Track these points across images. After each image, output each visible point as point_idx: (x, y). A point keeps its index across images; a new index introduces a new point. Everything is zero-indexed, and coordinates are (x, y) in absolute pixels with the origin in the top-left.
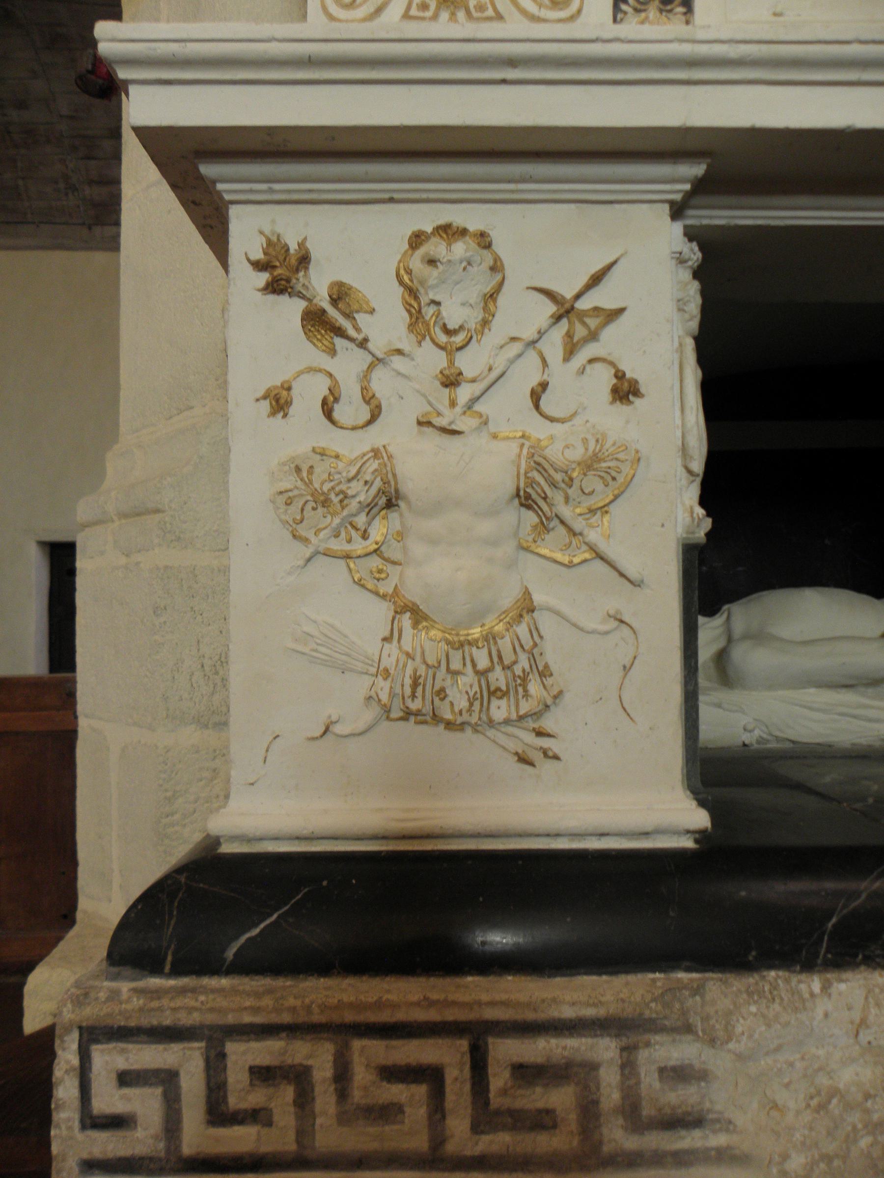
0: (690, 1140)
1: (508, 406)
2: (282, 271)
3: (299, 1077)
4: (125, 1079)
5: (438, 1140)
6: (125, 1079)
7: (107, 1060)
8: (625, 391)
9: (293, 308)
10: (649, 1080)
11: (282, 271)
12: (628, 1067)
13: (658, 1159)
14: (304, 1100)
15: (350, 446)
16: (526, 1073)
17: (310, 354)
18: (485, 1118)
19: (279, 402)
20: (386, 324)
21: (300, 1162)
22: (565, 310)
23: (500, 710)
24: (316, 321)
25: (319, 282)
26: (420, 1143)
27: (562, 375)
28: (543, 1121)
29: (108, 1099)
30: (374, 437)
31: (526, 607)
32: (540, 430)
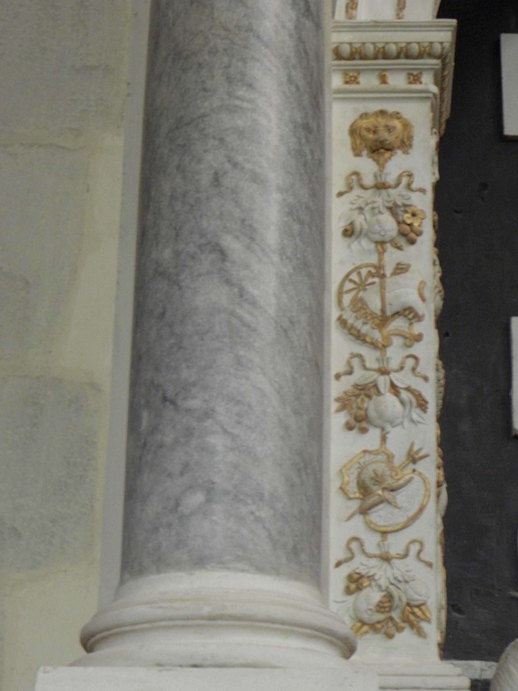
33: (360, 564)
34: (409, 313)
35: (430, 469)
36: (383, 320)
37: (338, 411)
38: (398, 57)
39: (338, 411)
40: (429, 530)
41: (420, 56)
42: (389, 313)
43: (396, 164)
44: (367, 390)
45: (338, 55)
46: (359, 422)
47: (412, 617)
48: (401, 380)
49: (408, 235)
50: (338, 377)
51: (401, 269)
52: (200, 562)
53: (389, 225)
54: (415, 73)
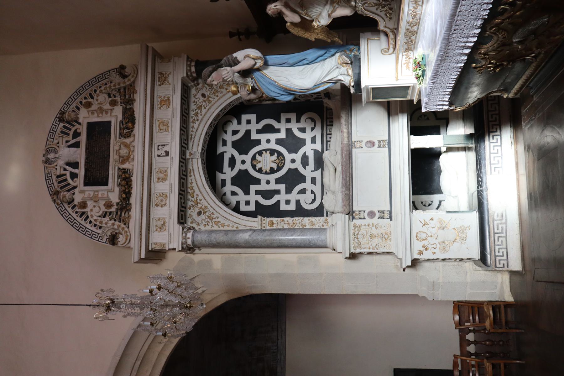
0: (504, 215)
1: (434, 231)
2: (421, 253)
3: (499, 249)
4: (500, 264)
5: (504, 237)
6: (500, 264)
7: (498, 265)
8: (432, 219)
9: (425, 252)
10: (498, 218)
11: (421, 253)
12: (497, 220)
13: (506, 217)
14: (501, 249)
15: (438, 246)
16: (498, 229)
17: (429, 250)
18: (502, 233)
19: (434, 253)
20: (426, 243)
21: (507, 249)
22: (424, 225)
23: (465, 231)
24: (426, 249)
25: (422, 249)
26: (505, 238)
27: (431, 225)
28: (502, 228)
29: (502, 265)
30: (437, 244)
31: (454, 229)
32: (436, 227)
33: (321, 225)
34: (293, 220)
35: (310, 218)
36: (294, 223)
40: (317, 218)
43: (275, 222)
44: (302, 225)
46: (305, 226)
47: (326, 220)
48: (300, 221)
49: (283, 220)
51: (287, 221)
52: (326, 238)
53: (283, 223)
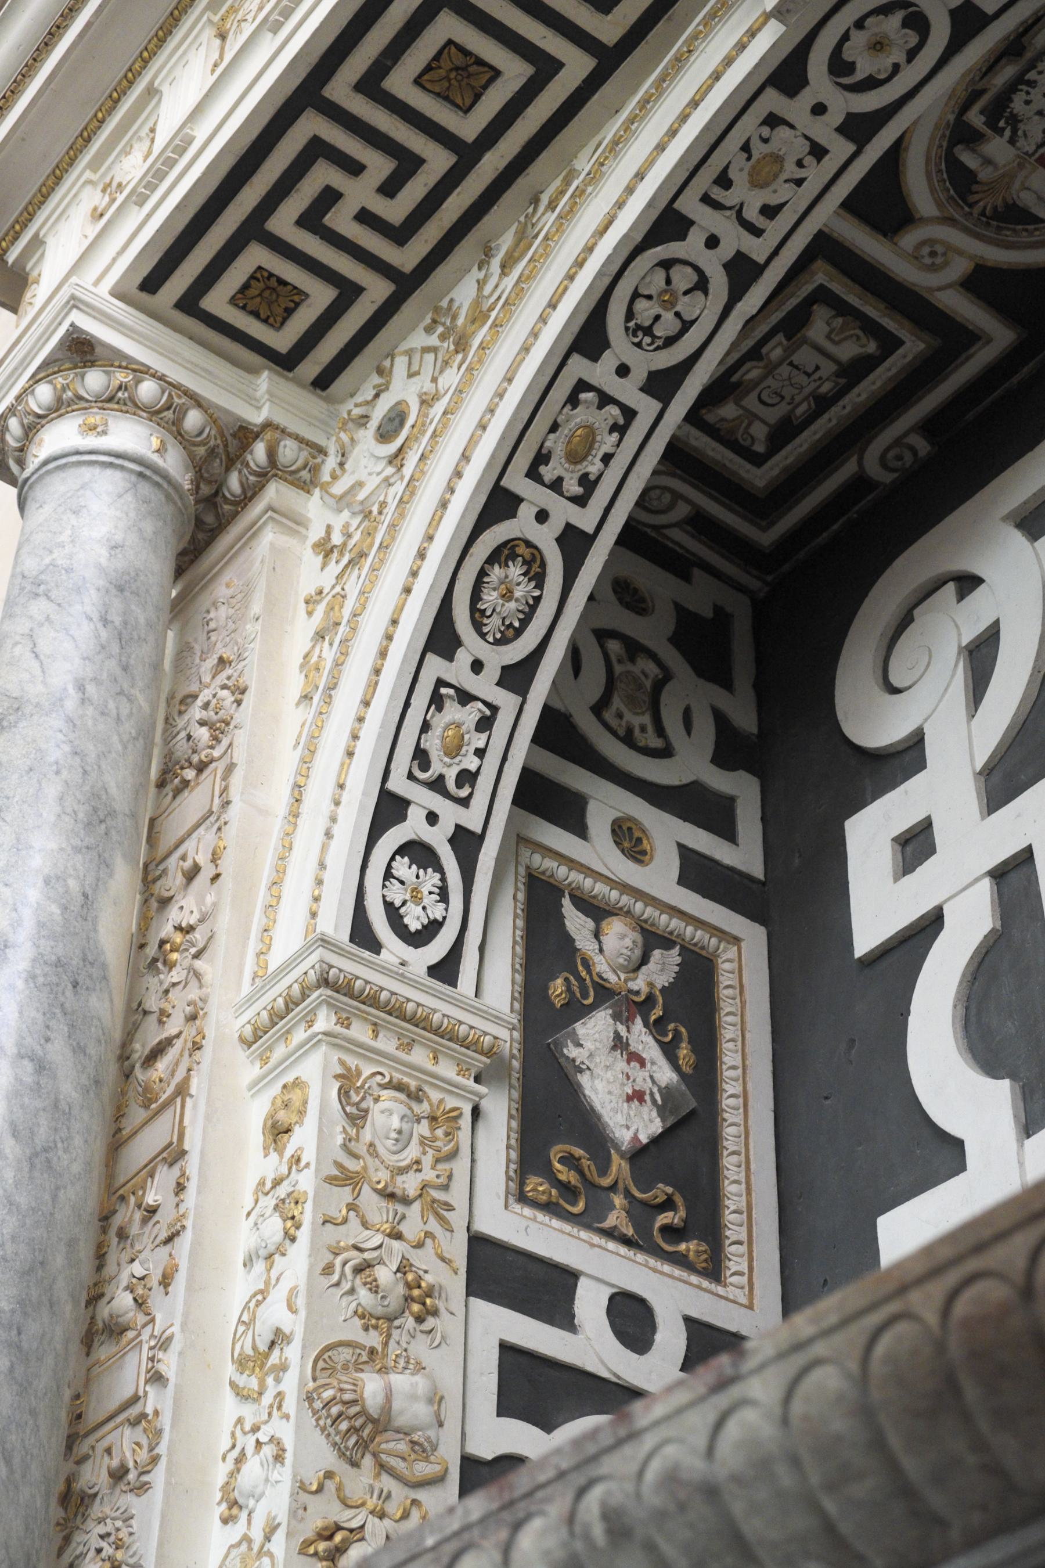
37: (219, 1503)
38: (288, 1010)
39: (219, 1503)
41: (304, 996)
42: (263, 1347)
45: (247, 1043)
50: (224, 1459)
54: (309, 1019)
